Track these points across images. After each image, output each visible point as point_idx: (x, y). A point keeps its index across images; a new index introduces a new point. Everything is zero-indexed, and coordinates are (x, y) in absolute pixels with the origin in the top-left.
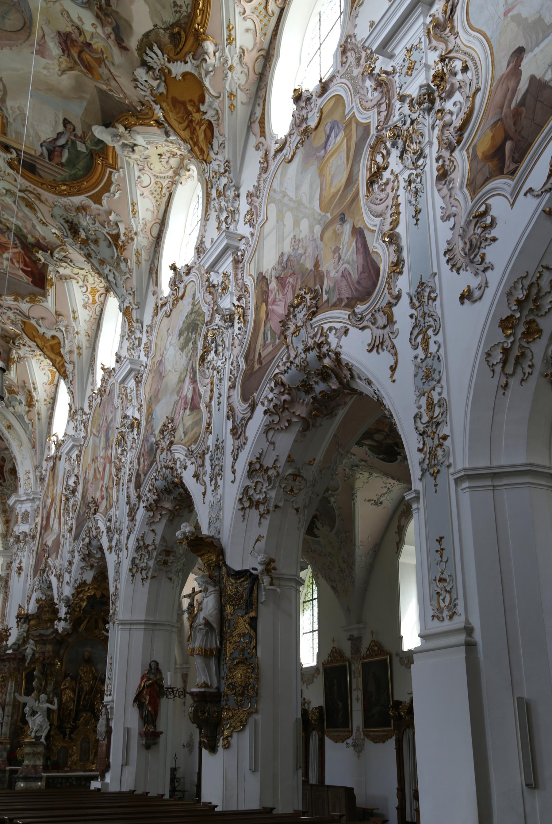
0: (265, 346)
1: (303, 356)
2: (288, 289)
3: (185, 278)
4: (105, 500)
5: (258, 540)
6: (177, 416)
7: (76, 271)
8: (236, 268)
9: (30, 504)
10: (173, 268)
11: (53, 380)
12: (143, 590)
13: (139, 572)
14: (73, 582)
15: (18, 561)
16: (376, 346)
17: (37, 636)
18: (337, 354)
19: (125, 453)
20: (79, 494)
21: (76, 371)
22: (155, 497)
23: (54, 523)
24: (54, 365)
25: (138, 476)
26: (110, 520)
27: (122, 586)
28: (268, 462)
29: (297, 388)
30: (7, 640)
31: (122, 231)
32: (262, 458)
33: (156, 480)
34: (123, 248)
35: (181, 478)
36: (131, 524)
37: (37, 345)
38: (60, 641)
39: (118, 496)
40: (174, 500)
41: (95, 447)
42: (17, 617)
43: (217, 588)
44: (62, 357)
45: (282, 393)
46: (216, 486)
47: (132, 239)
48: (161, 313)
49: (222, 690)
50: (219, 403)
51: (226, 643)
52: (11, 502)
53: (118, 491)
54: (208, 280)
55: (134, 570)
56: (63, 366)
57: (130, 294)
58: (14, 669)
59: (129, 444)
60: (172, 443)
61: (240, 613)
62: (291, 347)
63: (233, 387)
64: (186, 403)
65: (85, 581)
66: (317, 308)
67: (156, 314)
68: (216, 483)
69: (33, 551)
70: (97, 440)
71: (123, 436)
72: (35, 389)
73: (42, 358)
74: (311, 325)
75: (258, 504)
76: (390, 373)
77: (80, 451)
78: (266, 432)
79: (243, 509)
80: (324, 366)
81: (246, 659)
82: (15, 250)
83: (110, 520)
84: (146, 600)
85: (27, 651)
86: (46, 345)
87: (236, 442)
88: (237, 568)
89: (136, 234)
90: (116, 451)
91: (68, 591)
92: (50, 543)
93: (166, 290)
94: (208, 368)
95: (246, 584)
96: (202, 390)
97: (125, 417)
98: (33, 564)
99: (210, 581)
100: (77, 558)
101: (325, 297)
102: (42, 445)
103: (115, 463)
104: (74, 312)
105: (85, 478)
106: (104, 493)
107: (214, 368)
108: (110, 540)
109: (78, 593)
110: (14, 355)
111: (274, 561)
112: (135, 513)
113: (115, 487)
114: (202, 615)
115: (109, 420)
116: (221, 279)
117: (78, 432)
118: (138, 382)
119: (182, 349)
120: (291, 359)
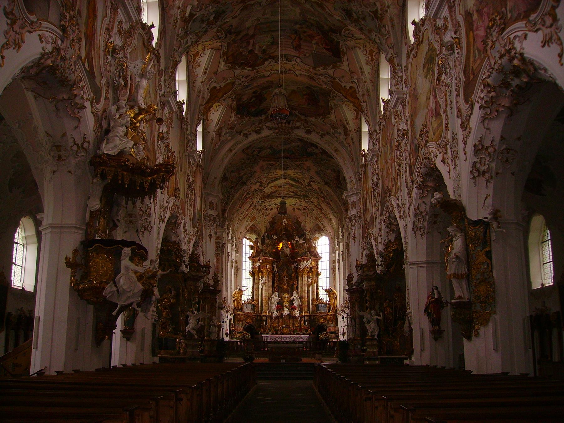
0: (475, 61)
1: (499, 62)
2: (485, 17)
3: (422, 29)
5: (486, 198)
6: (428, 123)
7: (357, 41)
8: (450, 12)
10: (414, 23)
11: (357, 115)
12: (423, 242)
14: (383, 242)
16: (546, 43)
18: (522, 54)
20: (380, 186)
24: (354, 106)
25: (410, 167)
26: (398, 199)
28: (487, 143)
29: (500, 86)
31: (379, 8)
32: (482, 141)
33: (421, 168)
34: (381, 19)
35: (435, 164)
36: (410, 199)
37: (343, 95)
39: (401, 183)
40: (433, 179)
43: (463, 233)
44: (358, 99)
45: (489, 92)
46: (456, 165)
47: (387, 11)
48: (411, 56)
49: (472, 300)
50: (451, 108)
51: (471, 270)
52: (344, 197)
53: (400, 179)
54: (435, 25)
57: (391, 48)
59: (403, 147)
60: (427, 142)
61: (479, 249)
62: (490, 58)
63: (458, 95)
64: (432, 113)
66: (505, 25)
67: (408, 58)
68: (455, 163)
70: (386, 149)
71: (399, 143)
72: (348, 123)
73: (348, 103)
74: (502, 38)
75: (484, 173)
76: (559, 59)
77: (378, 158)
78: (483, 122)
79: (474, 178)
80: (514, 66)
81: (486, 279)
82: (318, 37)
87: (464, 132)
88: (474, 219)
89: (388, 7)
90: (396, 153)
91: (381, 248)
92: (368, 220)
93: (412, 40)
94: (443, 86)
95: (482, 229)
96: (441, 102)
97: (399, 130)
99: (457, 229)
101: (509, 15)
103: (397, 162)
104: (361, 69)
105: (382, 175)
106: (393, 182)
107: (446, 85)
108: (400, 212)
109: (387, 248)
110: (331, 103)
111: (499, 211)
112: (412, 192)
113: (399, 177)
114: (454, 252)
115: (391, 135)
116: (442, 22)
118: (403, 106)
119: (426, 77)
120: (492, 66)
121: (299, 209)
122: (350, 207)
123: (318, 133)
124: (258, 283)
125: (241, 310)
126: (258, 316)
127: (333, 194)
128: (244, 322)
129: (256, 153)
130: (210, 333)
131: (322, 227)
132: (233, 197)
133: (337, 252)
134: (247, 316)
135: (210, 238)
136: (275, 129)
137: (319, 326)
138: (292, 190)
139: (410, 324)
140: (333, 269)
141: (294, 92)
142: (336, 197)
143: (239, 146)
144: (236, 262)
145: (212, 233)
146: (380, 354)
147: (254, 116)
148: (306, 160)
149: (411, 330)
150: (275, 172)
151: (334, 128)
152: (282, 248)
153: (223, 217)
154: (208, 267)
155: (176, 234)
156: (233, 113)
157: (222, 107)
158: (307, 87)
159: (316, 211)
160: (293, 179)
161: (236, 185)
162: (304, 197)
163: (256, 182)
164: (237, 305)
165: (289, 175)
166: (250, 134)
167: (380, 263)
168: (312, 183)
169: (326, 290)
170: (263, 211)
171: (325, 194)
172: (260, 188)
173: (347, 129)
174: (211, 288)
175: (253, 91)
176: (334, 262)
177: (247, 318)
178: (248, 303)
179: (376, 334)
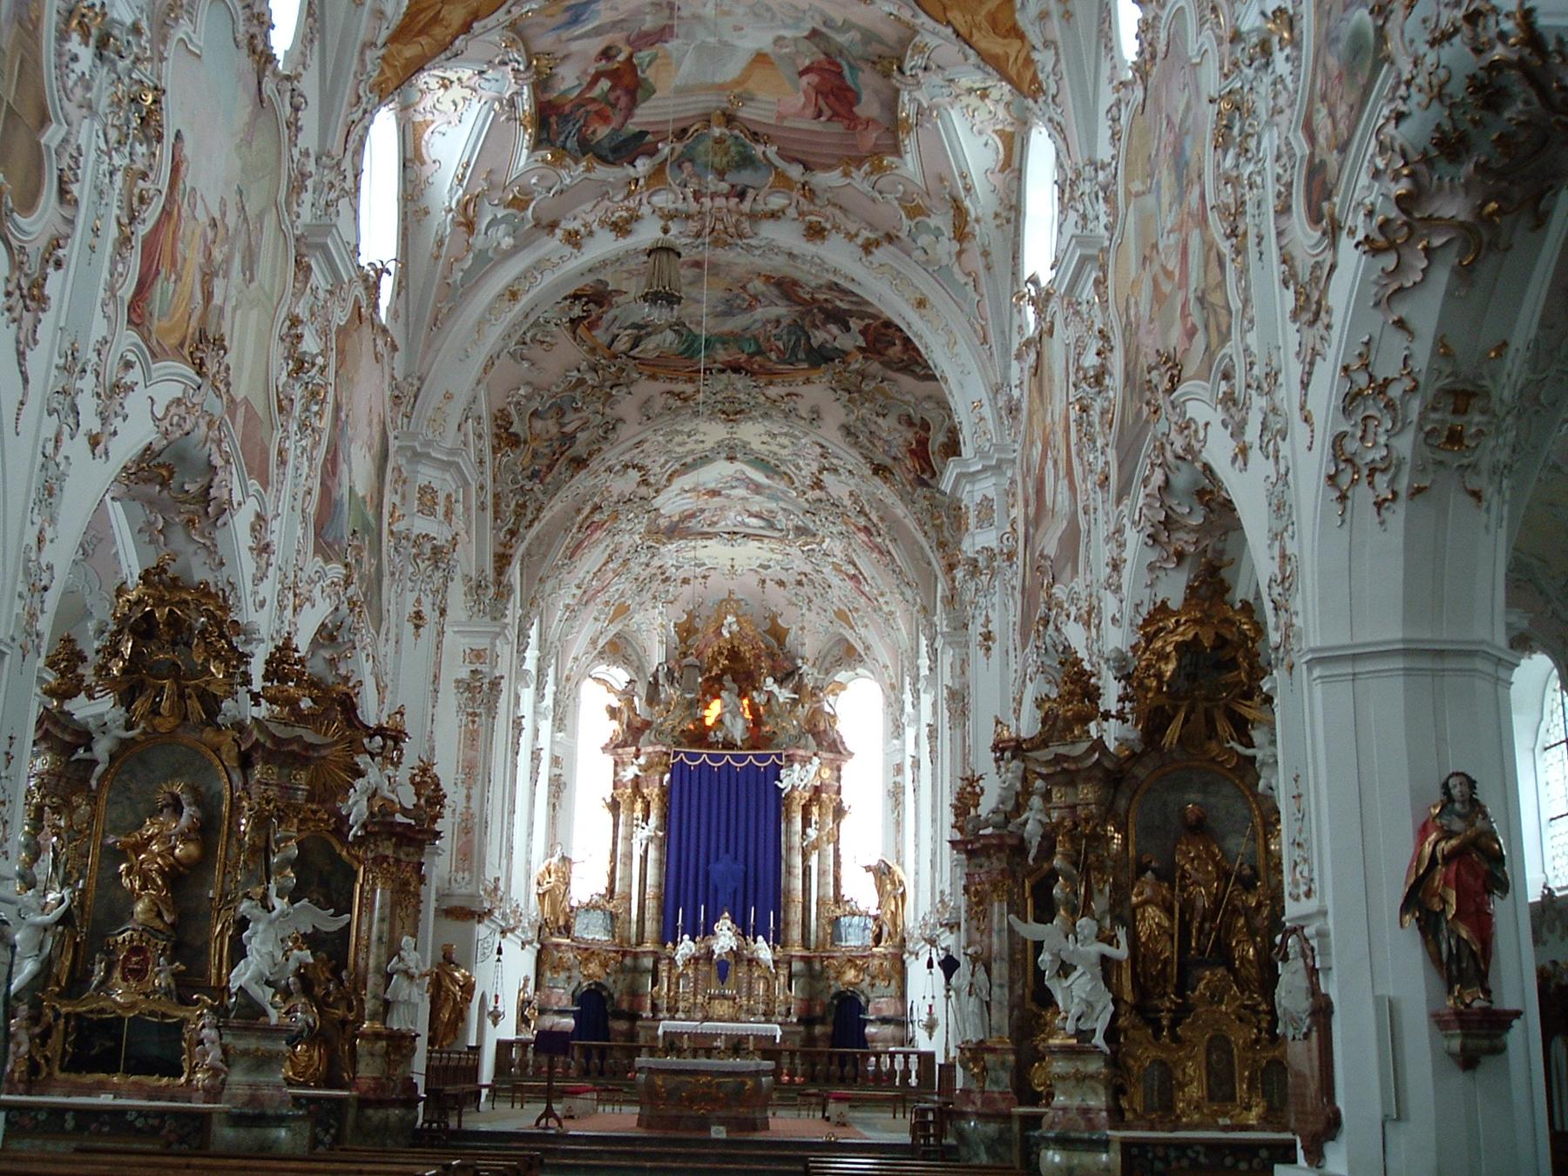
4: (1200, 339)
9: (993, 480)
12: (1385, 541)
13: (1364, 482)
14: (1128, 608)
15: (981, 620)
17: (1048, 763)
19: (1252, 143)
20: (1115, 381)
21: (1063, 65)
22: (1402, 187)
23: (1058, 495)
25: (1315, 171)
26: (1226, 376)
27: (1306, 543)
30: (977, 806)
38: (1114, 775)
41: (1145, 222)
42: (995, 748)
44: (1021, 36)
52: (946, 484)
55: (1344, 481)
56: (1029, 61)
58: (1003, 871)
59: (1262, 110)
65: (1164, 603)
69: (1013, 588)
71: (1236, 106)
72: (968, 190)
83: (1226, 376)
84: (1399, 576)
85: (1028, 827)
86: (978, 19)
92: (1051, 549)
98: (1018, 619)
100: (1133, 537)
102: (1003, 332)
106: (1196, 317)
109: (1149, 639)
110: (907, 110)
115: (1177, 120)
117: (1090, 226)
121: (781, 583)
122: (972, 521)
123: (851, 237)
124: (629, 838)
125: (567, 929)
126: (624, 954)
127: (900, 510)
128: (575, 973)
129: (622, 345)
130: (387, 1005)
131: (860, 648)
132: (539, 509)
133: (910, 733)
134: (588, 952)
135: (417, 627)
136: (688, 217)
137: (840, 995)
138: (755, 509)
139: (1313, 972)
140: (896, 794)
141: (760, 58)
142: (911, 523)
143: (549, 278)
144: (556, 761)
145: (426, 610)
146: (1117, 1116)
147: (604, 160)
148: (808, 381)
149: (1322, 1011)
150: (697, 432)
151: (914, 211)
152: (720, 720)
153: (499, 583)
154: (394, 736)
155: (211, 550)
156: (525, 138)
157: (476, 106)
158: (814, 33)
159: (841, 588)
160: (760, 463)
161: (550, 468)
162: (797, 536)
163: (626, 467)
164: (554, 912)
165: (745, 445)
166: (591, 234)
167: (1114, 707)
168: (825, 476)
169: (868, 869)
170: (654, 585)
171: (875, 519)
172: (643, 491)
173: (967, 213)
174: (399, 818)
175: (597, 44)
176: (899, 769)
177: (586, 961)
178: (590, 907)
179: (1101, 1026)
